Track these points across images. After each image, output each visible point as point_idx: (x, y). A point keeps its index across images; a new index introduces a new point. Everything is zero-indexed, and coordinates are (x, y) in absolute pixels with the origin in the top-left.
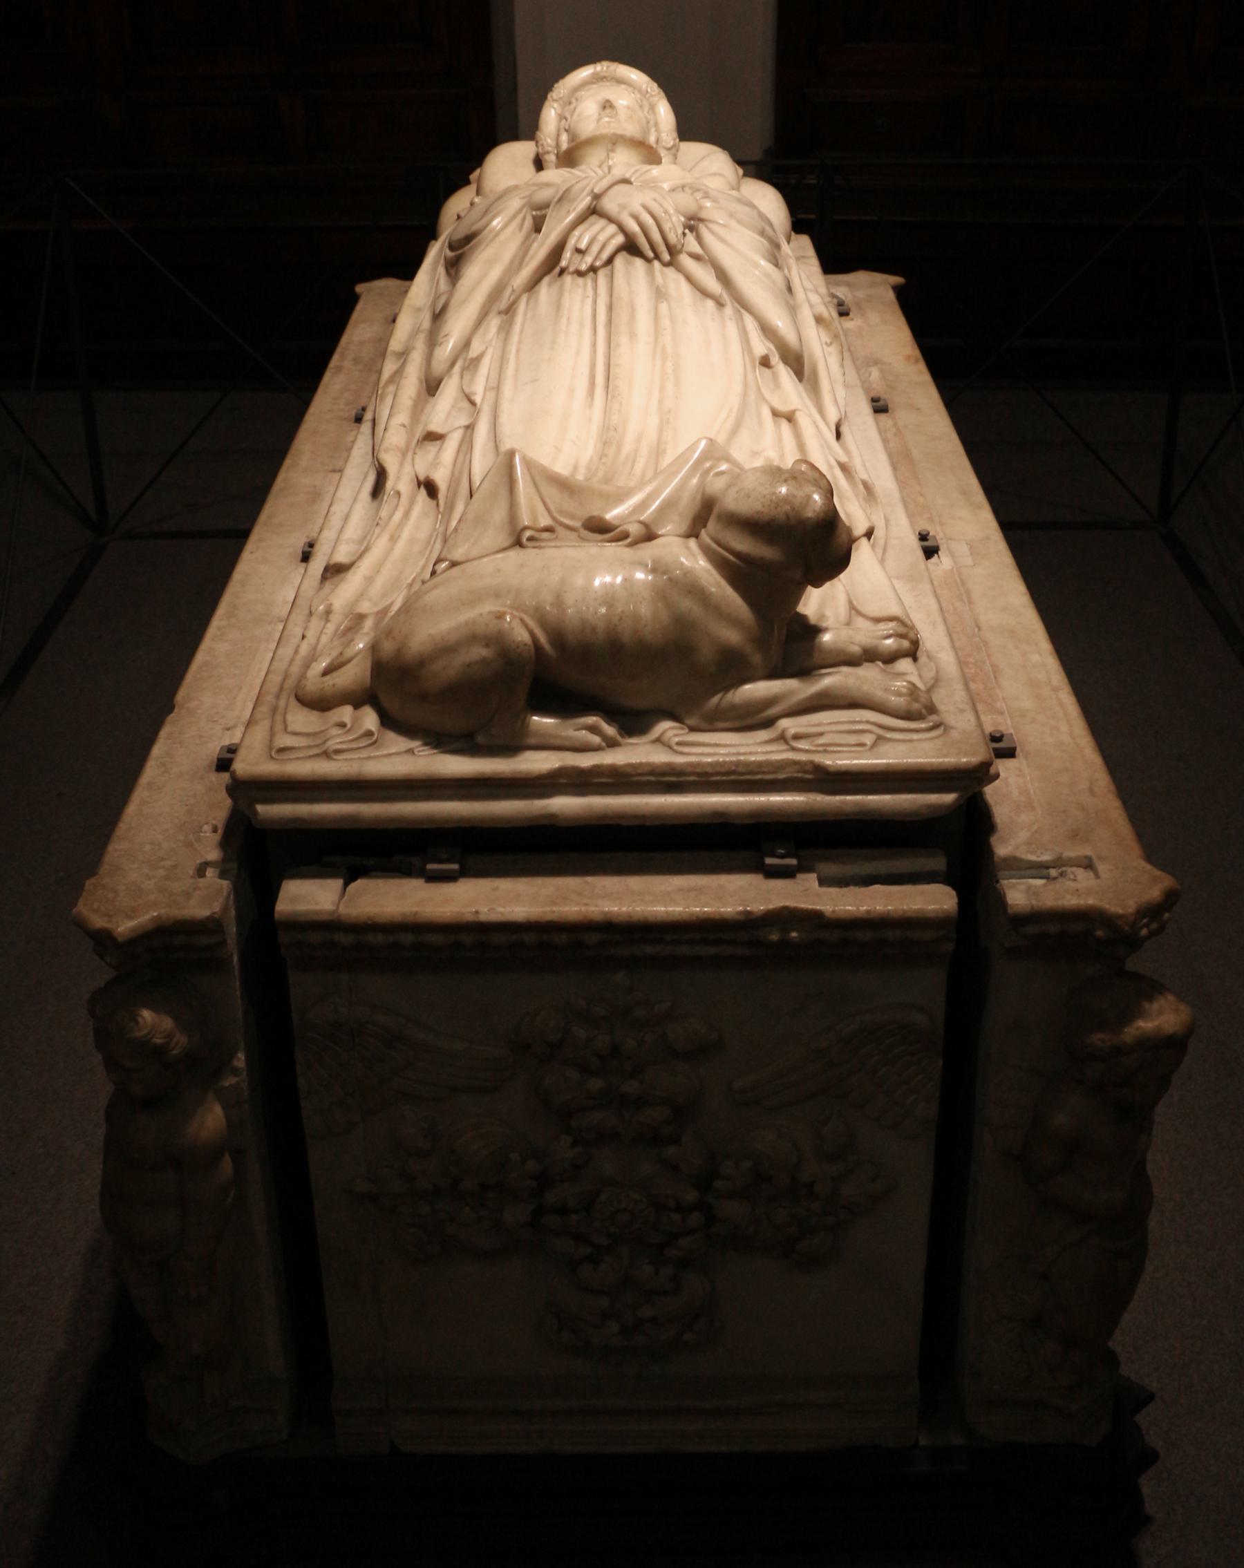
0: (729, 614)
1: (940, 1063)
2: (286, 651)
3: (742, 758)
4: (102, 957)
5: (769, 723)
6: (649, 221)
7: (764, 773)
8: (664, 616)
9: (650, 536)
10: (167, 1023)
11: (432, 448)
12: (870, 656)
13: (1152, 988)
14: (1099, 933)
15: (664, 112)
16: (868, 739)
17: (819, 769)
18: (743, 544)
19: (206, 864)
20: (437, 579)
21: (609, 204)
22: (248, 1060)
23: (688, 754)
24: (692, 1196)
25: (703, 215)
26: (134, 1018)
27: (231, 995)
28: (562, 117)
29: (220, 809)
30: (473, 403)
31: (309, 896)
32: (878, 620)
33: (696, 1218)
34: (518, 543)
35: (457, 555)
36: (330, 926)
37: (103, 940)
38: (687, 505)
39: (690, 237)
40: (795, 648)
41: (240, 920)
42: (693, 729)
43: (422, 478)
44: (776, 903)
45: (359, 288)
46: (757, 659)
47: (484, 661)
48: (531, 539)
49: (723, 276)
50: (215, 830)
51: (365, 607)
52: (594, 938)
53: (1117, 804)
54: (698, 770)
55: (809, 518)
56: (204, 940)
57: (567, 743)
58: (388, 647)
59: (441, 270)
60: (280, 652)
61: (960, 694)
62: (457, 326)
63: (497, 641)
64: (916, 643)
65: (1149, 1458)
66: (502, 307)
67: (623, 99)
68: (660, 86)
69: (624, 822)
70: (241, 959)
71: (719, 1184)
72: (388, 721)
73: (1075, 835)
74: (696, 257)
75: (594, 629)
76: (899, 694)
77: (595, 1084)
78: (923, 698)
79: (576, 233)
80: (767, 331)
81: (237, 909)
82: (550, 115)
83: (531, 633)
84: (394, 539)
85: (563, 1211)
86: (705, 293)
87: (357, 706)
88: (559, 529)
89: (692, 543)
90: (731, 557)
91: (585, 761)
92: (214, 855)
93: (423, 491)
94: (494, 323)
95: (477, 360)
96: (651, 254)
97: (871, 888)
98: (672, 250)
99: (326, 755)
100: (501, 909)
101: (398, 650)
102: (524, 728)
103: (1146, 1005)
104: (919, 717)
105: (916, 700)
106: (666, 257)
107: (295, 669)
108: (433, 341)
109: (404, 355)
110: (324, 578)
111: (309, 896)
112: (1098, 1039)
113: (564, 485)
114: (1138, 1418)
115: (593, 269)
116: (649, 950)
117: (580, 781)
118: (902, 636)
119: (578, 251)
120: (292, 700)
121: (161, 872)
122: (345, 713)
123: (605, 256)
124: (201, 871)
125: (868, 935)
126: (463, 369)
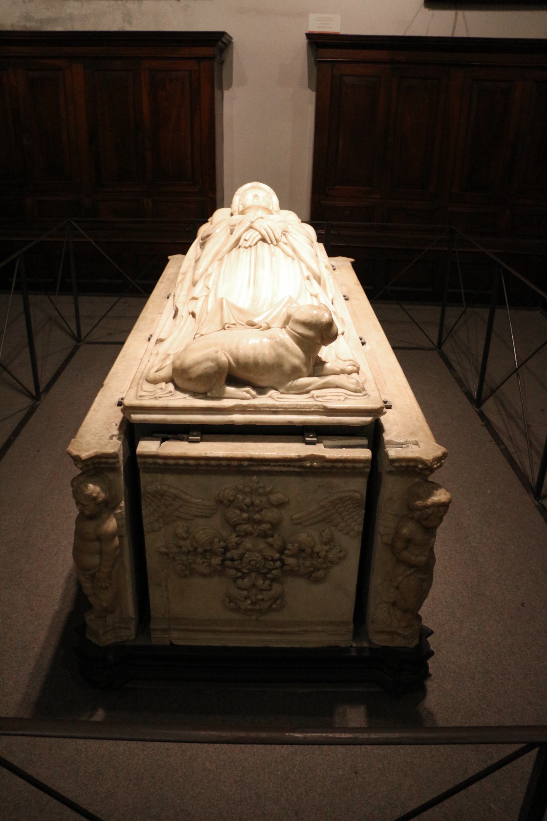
0: (295, 355)
1: (364, 511)
2: (143, 366)
4: (76, 465)
5: (308, 392)
6: (270, 231)
8: (273, 354)
9: (269, 328)
10: (98, 489)
11: (194, 302)
12: (343, 372)
13: (437, 487)
14: (420, 466)
15: (275, 200)
16: (342, 398)
17: (325, 408)
18: (302, 330)
19: (113, 435)
20: (195, 340)
21: (256, 225)
22: (125, 503)
24: (277, 556)
25: (288, 230)
26: (86, 487)
27: (120, 481)
28: (240, 200)
29: (118, 416)
30: (208, 288)
31: (147, 447)
32: (345, 361)
33: (278, 563)
34: (224, 329)
35: (202, 332)
36: (155, 457)
37: (76, 459)
38: (282, 318)
39: (284, 237)
40: (317, 367)
41: (124, 455)
42: (282, 393)
43: (190, 311)
45: (170, 257)
46: (304, 370)
47: (211, 367)
48: (228, 327)
49: (294, 250)
50: (116, 425)
51: (170, 352)
52: (246, 463)
53: (426, 424)
56: (112, 461)
57: (239, 397)
58: (178, 363)
59: (198, 247)
60: (140, 366)
61: (373, 385)
62: (203, 263)
63: (215, 360)
64: (358, 368)
65: (431, 654)
66: (219, 258)
67: (261, 194)
68: (275, 190)
70: (124, 469)
71: (287, 552)
72: (177, 388)
73: (412, 434)
74: (286, 244)
75: (249, 357)
76: (353, 384)
77: (245, 515)
78: (361, 386)
79: (245, 234)
80: (309, 268)
81: (123, 451)
82: (236, 199)
83: (227, 358)
84: (180, 331)
85: (232, 560)
86: (288, 255)
88: (238, 325)
89: (283, 329)
90: (297, 335)
91: (245, 403)
92: (116, 432)
93: (191, 315)
94: (216, 263)
95: (210, 275)
96: (270, 242)
98: (277, 241)
99: (156, 398)
100: (214, 452)
101: (182, 364)
102: (224, 392)
103: (435, 492)
104: (360, 392)
105: (359, 386)
106: (275, 243)
107: (146, 372)
108: (195, 269)
109: (184, 274)
110: (156, 343)
111: (147, 447)
112: (419, 503)
113: (240, 310)
114: (428, 639)
115: (250, 246)
116: (265, 468)
117: (243, 410)
118: (354, 366)
119: (246, 240)
120: (145, 380)
121: (97, 438)
122: (163, 385)
123: (255, 242)
124: (111, 438)
125: (340, 465)
126: (205, 278)
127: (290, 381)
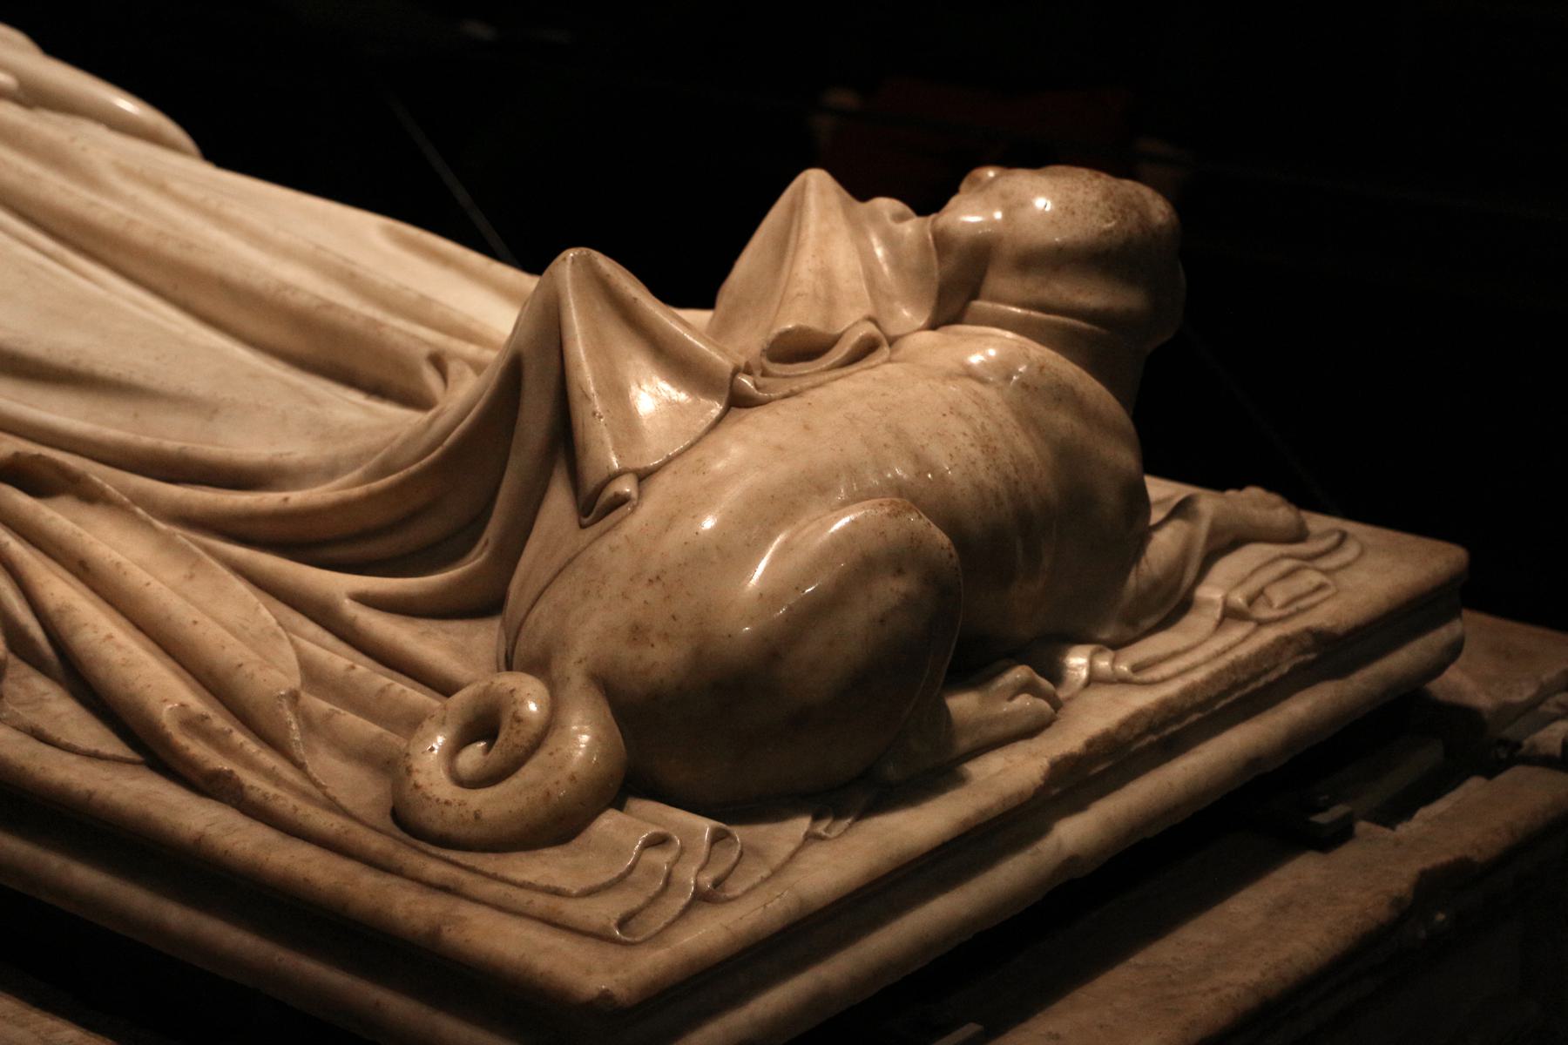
3: (1231, 657)
7: (1266, 672)
18: (1093, 295)
23: (1164, 680)
42: (1116, 645)
44: (1401, 878)
47: (908, 601)
54: (1199, 698)
55: (1160, 227)
57: (1014, 727)
87: (619, 805)
97: (1417, 816)
101: (698, 653)
122: (608, 822)
127: (1128, 571)
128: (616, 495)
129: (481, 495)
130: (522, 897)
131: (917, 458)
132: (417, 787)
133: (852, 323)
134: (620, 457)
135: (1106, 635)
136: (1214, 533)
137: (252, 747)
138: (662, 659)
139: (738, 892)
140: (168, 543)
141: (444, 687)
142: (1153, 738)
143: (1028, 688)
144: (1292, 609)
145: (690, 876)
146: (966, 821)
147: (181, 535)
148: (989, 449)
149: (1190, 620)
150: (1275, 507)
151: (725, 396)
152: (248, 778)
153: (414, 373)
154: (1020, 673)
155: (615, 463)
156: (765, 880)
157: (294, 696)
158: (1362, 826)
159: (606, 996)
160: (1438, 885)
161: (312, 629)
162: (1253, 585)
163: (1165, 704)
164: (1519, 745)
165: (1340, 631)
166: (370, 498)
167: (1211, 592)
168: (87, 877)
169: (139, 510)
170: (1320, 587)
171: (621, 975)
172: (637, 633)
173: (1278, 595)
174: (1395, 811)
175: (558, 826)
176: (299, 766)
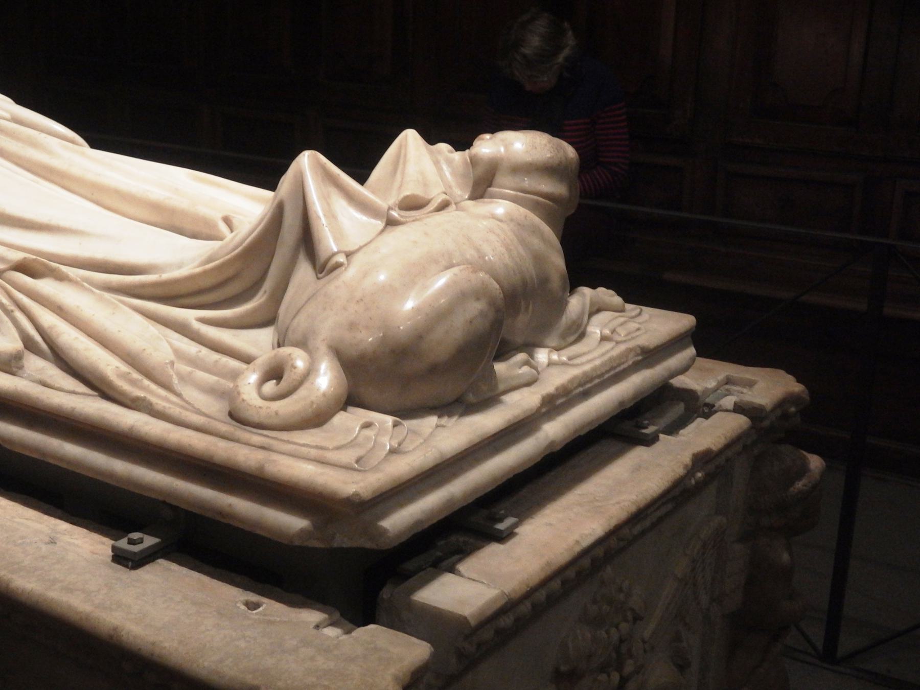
7: (623, 363)
23: (582, 364)
42: (558, 349)
47: (482, 314)
54: (599, 373)
57: (522, 381)
69: (582, 433)
87: (344, 409)
90: (541, 199)
128: (337, 263)
129: (249, 280)
130: (304, 450)
131: (478, 250)
132: (243, 400)
133: (437, 195)
134: (337, 245)
135: (554, 344)
136: (592, 304)
137: (153, 387)
138: (367, 339)
139: (411, 449)
140: (101, 299)
141: (247, 360)
142: (581, 389)
143: (527, 363)
144: (629, 337)
145: (387, 443)
146: (509, 420)
147: (107, 295)
148: (509, 250)
149: (585, 341)
150: (612, 296)
151: (385, 220)
152: (154, 400)
153: (215, 226)
154: (521, 357)
155: (335, 250)
156: (421, 444)
157: (172, 363)
158: (661, 436)
159: (356, 494)
160: (702, 459)
161: (176, 336)
162: (611, 326)
163: (585, 374)
164: (714, 406)
165: (652, 346)
166: (205, 273)
167: (595, 329)
168: (72, 450)
169: (86, 284)
170: (638, 329)
171: (362, 484)
172: (352, 326)
173: (622, 332)
174: (673, 429)
175: (317, 419)
176: (179, 395)
